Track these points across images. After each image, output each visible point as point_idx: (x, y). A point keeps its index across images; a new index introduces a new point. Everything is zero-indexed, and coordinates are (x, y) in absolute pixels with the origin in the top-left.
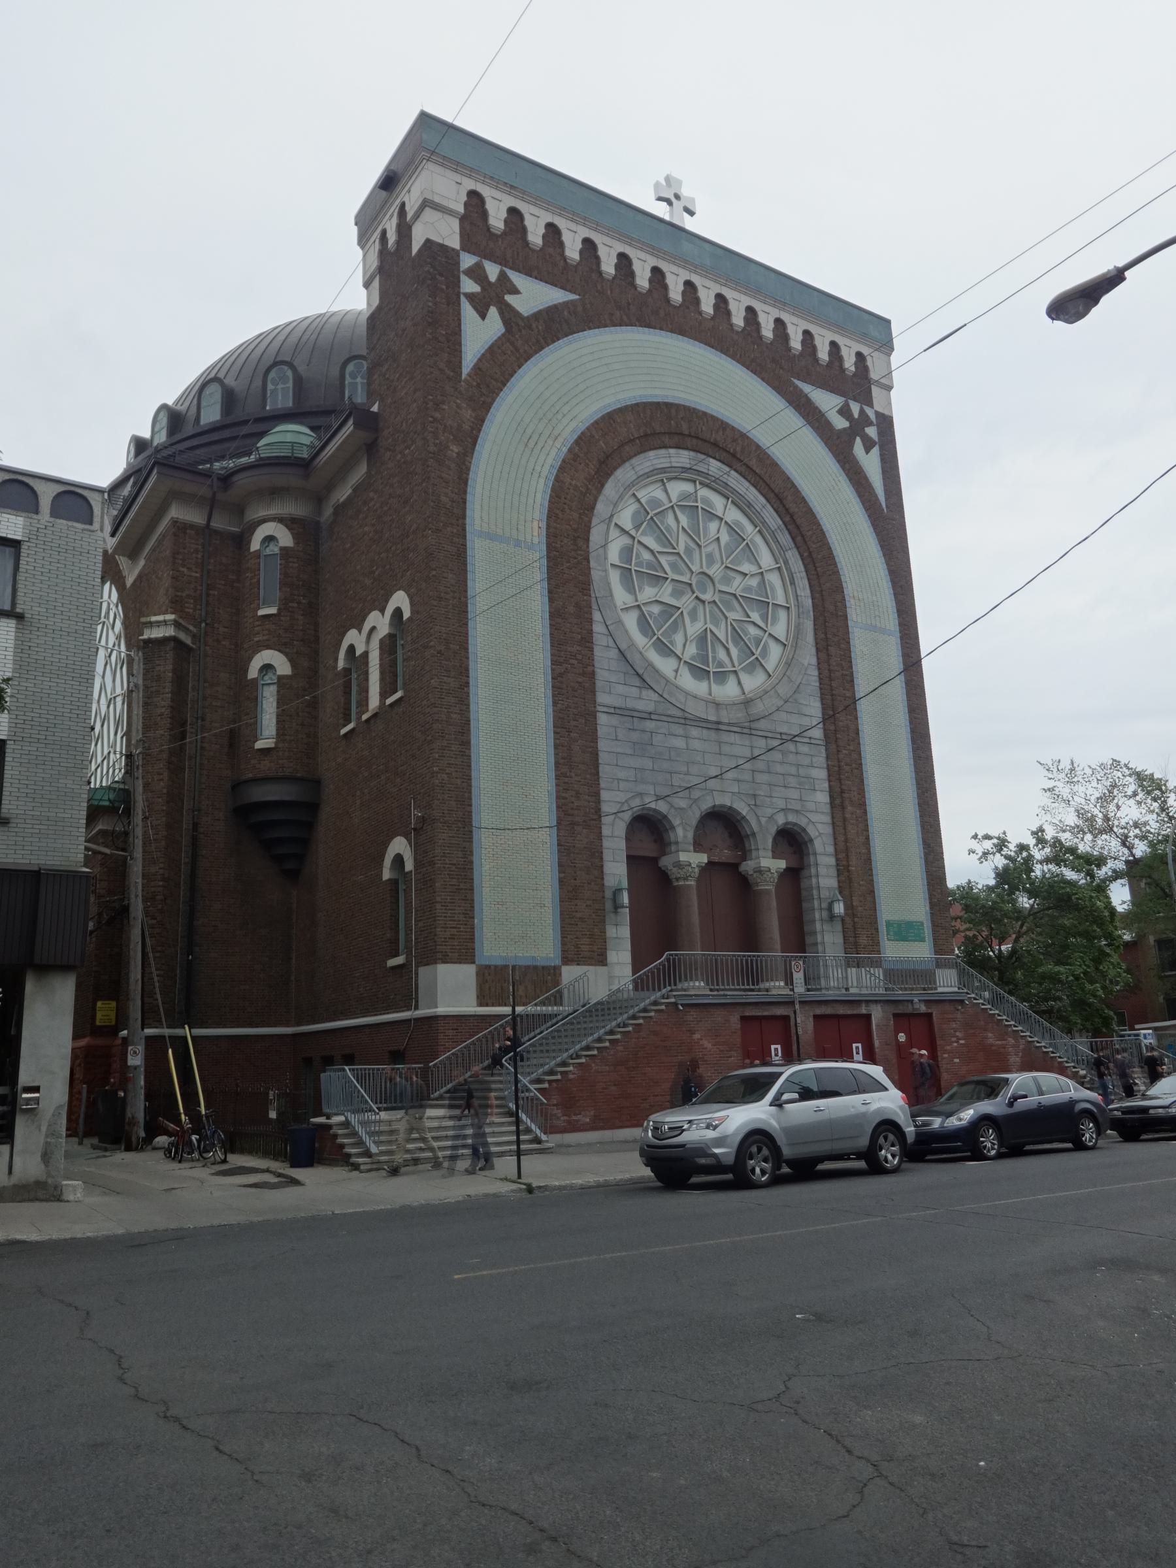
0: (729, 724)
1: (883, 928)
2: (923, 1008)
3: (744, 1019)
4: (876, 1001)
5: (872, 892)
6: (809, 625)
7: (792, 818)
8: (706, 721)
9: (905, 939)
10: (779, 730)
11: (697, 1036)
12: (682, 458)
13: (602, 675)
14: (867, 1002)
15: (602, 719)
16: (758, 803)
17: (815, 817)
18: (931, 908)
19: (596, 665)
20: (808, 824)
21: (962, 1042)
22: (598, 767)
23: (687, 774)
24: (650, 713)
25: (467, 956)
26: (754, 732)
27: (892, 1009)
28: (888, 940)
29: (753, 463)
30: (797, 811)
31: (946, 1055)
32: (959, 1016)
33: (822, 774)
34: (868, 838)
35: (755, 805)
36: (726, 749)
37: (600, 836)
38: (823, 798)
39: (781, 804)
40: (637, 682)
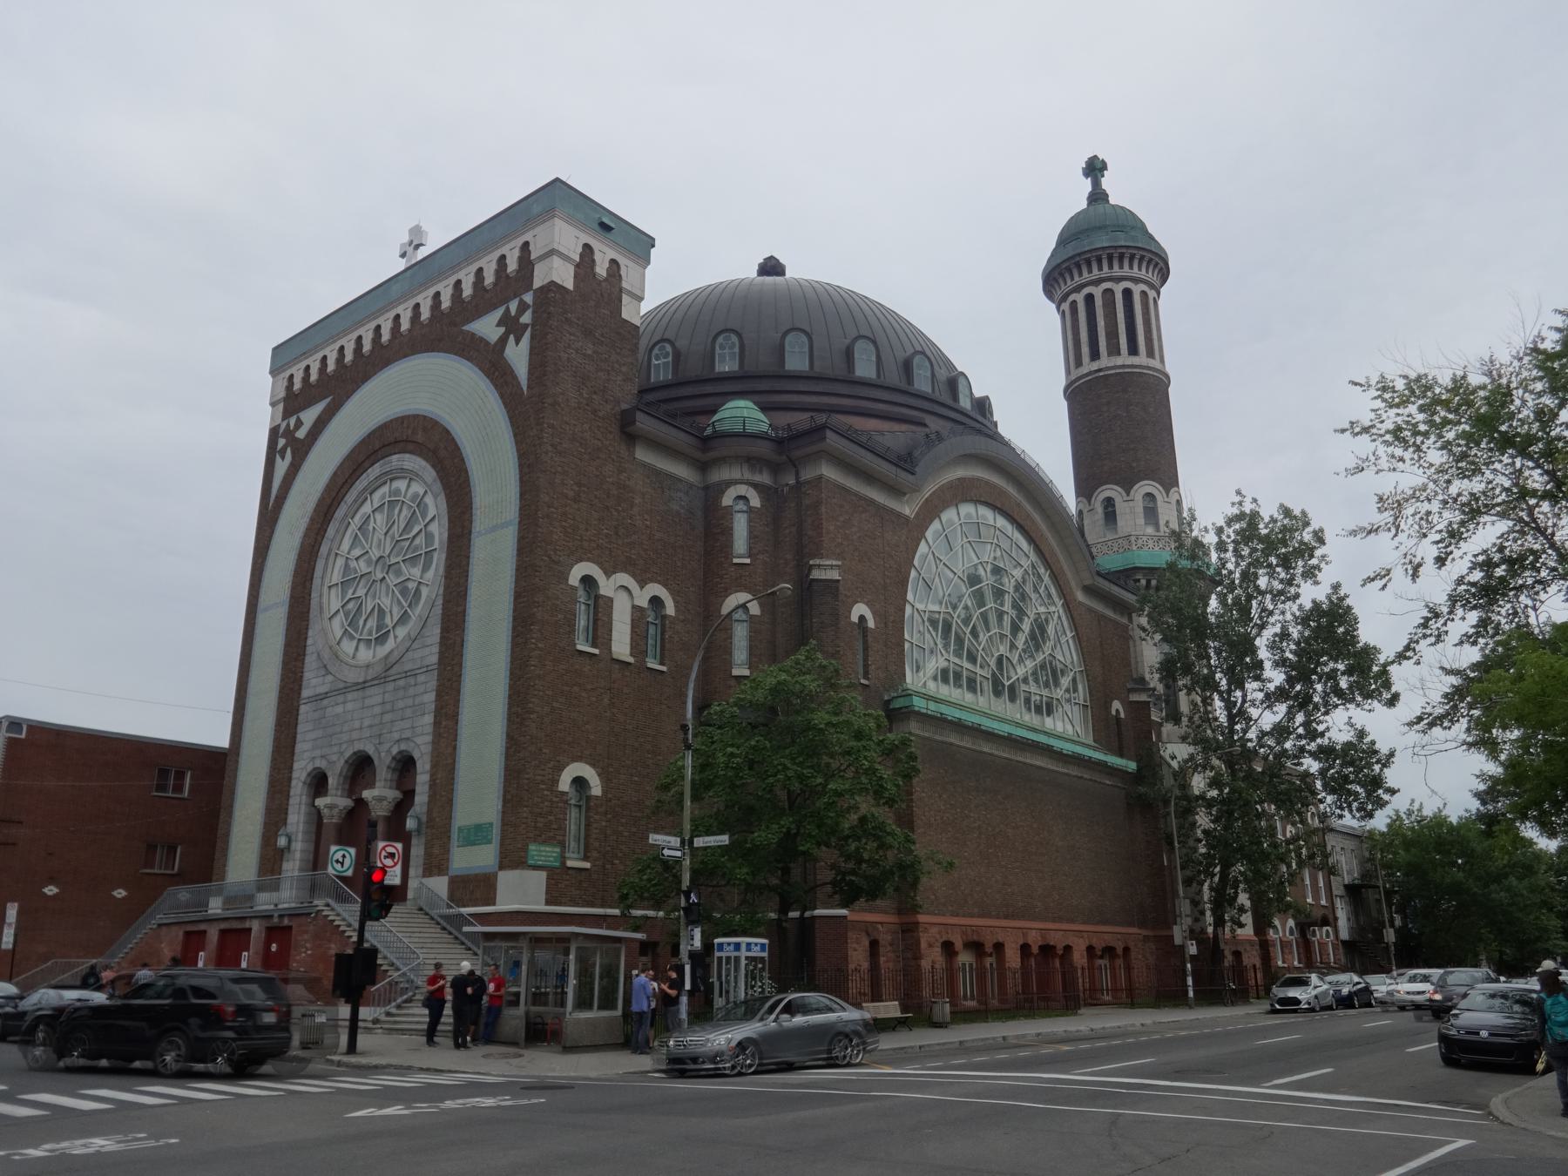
0: (373, 680)
2: (286, 922)
3: (188, 934)
4: (256, 917)
5: (450, 802)
6: (444, 556)
7: (403, 747)
8: (358, 684)
9: (473, 844)
10: (406, 669)
11: (163, 945)
12: (375, 471)
13: (307, 675)
14: (251, 917)
15: (303, 709)
17: (419, 740)
18: (504, 806)
19: (305, 670)
21: (309, 952)
22: (294, 747)
23: (341, 732)
24: (327, 693)
25: (219, 892)
26: (388, 679)
27: (266, 924)
28: (458, 846)
29: (420, 438)
30: (408, 739)
31: (295, 965)
32: (311, 927)
33: (431, 697)
34: (455, 748)
36: (368, 702)
37: (288, 797)
38: (429, 719)
39: (396, 736)
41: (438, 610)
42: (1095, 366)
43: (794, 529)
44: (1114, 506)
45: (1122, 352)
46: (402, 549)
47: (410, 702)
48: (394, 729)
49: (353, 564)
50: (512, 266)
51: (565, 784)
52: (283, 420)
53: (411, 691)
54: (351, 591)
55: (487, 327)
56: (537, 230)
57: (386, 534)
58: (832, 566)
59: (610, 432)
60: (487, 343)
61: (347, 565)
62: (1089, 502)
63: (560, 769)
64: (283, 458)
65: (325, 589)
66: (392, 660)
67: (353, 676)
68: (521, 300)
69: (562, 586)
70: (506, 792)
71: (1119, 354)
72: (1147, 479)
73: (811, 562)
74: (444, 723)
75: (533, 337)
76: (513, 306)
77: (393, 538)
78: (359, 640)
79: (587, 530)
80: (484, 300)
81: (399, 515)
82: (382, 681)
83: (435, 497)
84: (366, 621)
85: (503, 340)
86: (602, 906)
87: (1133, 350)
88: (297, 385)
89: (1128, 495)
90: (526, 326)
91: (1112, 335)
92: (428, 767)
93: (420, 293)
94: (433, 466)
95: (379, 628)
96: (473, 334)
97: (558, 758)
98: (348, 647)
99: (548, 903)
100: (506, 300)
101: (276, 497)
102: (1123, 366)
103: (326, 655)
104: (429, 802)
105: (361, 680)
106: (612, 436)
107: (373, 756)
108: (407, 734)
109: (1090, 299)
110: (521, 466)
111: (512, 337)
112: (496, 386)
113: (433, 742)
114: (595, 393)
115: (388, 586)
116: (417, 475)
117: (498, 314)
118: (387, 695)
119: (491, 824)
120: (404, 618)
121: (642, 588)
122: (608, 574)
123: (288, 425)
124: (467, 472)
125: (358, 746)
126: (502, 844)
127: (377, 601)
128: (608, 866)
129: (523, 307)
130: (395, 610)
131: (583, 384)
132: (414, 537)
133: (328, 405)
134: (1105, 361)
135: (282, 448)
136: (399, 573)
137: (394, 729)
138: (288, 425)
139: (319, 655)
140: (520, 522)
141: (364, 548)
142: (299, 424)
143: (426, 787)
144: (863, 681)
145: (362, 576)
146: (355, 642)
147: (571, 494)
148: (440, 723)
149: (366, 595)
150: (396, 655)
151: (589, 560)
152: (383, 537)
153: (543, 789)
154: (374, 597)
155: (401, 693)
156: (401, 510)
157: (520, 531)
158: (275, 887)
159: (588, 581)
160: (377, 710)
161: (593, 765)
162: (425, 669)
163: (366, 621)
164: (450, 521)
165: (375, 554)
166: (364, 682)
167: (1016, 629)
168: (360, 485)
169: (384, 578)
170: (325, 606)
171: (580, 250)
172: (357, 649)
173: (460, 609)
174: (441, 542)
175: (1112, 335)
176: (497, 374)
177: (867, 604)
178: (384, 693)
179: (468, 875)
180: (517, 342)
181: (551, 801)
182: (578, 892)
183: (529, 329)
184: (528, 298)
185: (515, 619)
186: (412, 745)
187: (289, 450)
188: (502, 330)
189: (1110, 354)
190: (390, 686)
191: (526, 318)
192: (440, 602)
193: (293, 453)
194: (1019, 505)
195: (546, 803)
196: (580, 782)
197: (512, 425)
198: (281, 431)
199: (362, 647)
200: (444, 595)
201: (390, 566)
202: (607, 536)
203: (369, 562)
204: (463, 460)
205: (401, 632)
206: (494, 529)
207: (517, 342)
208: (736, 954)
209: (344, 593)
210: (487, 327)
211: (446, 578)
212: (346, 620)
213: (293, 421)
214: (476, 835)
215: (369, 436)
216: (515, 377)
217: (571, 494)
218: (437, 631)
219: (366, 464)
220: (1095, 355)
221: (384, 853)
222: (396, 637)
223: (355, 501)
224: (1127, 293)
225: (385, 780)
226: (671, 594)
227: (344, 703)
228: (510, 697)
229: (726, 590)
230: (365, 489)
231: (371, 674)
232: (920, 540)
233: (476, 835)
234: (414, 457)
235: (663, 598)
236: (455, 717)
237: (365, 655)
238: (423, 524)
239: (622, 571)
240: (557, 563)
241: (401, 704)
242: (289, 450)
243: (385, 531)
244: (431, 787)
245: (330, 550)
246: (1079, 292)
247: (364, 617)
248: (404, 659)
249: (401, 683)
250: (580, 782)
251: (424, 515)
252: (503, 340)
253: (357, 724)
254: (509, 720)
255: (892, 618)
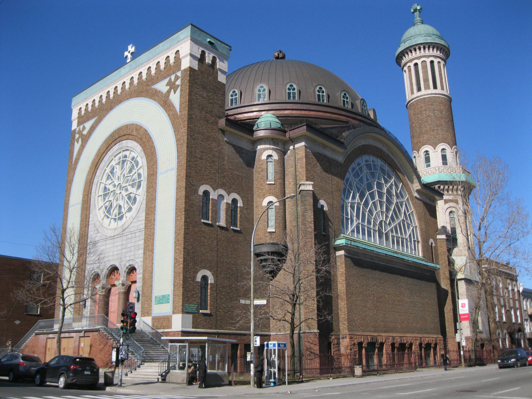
1: (153, 299)
6: (146, 183)
7: (131, 263)
8: (111, 237)
10: (131, 231)
16: (122, 260)
17: (138, 260)
18: (174, 288)
19: (89, 231)
20: (135, 264)
26: (124, 235)
28: (155, 304)
29: (134, 133)
30: (133, 260)
34: (153, 263)
35: (121, 262)
36: (116, 244)
38: (141, 251)
39: (128, 258)
40: (96, 232)
41: (144, 206)
42: (419, 94)
43: (293, 169)
44: (429, 154)
45: (431, 88)
46: (128, 180)
47: (133, 244)
48: (127, 256)
49: (108, 187)
50: (172, 60)
51: (199, 278)
52: (77, 127)
53: (133, 240)
54: (107, 198)
55: (162, 86)
56: (182, 46)
57: (121, 174)
58: (309, 184)
59: (214, 129)
60: (162, 93)
61: (105, 188)
62: (418, 153)
63: (196, 272)
64: (78, 142)
65: (97, 197)
66: (125, 227)
67: (110, 234)
68: (176, 75)
69: (195, 195)
70: (175, 282)
71: (429, 89)
72: (444, 143)
73: (300, 183)
74: (148, 253)
75: (181, 90)
76: (173, 77)
77: (124, 176)
78: (111, 218)
79: (205, 171)
80: (160, 75)
81: (126, 166)
82: (122, 235)
83: (142, 158)
84: (114, 210)
85: (169, 92)
86: (216, 329)
87: (435, 87)
88: (83, 112)
89: (435, 149)
90: (179, 86)
91: (426, 80)
92: (141, 271)
93: (133, 73)
94: (141, 145)
95: (119, 213)
96: (156, 90)
97: (196, 267)
98: (106, 221)
99: (193, 328)
100: (169, 75)
101: (76, 159)
102: (432, 94)
103: (98, 224)
104: (143, 286)
105: (112, 235)
106: (215, 131)
107: (118, 267)
108: (132, 258)
109: (416, 65)
110: (177, 145)
111: (172, 90)
112: (166, 111)
113: (143, 261)
114: (207, 113)
115: (123, 196)
116: (134, 149)
117: (166, 81)
118: (123, 241)
119: (169, 295)
120: (130, 209)
121: (229, 195)
122: (214, 189)
123: (80, 129)
124: (155, 148)
125: (112, 263)
126: (174, 302)
127: (118, 202)
128: (218, 313)
129: (177, 78)
130: (126, 205)
131: (203, 109)
132: (133, 175)
133: (96, 120)
134: (423, 92)
135: (77, 138)
136: (127, 190)
137: (127, 256)
138: (80, 129)
139: (95, 224)
140: (177, 169)
141: (112, 180)
142: (84, 128)
143: (141, 280)
144: (323, 233)
145: (112, 192)
146: (110, 219)
147: (199, 156)
148: (146, 253)
149: (113, 199)
150: (127, 225)
151: (206, 184)
152: (120, 175)
153: (190, 281)
154: (117, 200)
155: (129, 241)
156: (127, 164)
157: (178, 172)
158: (80, 320)
159: (206, 193)
160: (120, 248)
161: (211, 271)
162: (139, 231)
163: (114, 210)
164: (148, 169)
165: (117, 183)
166: (114, 236)
167: (388, 210)
168: (110, 153)
169: (121, 192)
170: (97, 204)
171: (200, 53)
172: (110, 222)
173: (153, 205)
174: (144, 177)
175: (426, 80)
176: (166, 106)
177: (324, 200)
178: (122, 240)
179: (160, 317)
180: (175, 92)
181: (194, 286)
182: (205, 323)
183: (180, 87)
184: (179, 74)
185: (176, 209)
186: (135, 262)
187: (80, 139)
188: (168, 87)
189: (426, 89)
190: (125, 238)
191: (178, 82)
192: (145, 202)
193: (82, 141)
194: (388, 156)
195: (191, 286)
196: (205, 278)
197: (173, 127)
198: (77, 131)
199: (112, 221)
200: (146, 200)
201: (123, 187)
202: (214, 173)
203: (115, 186)
204: (153, 143)
205: (128, 215)
206: (167, 171)
207: (175, 92)
208: (274, 348)
209: (104, 199)
210: (162, 86)
211: (147, 192)
212: (106, 210)
213: (81, 127)
214: (162, 300)
215: (113, 133)
216: (174, 107)
217: (199, 156)
218: (144, 214)
219: (112, 145)
220: (419, 89)
221: (129, 307)
222: (126, 217)
223: (108, 160)
224: (432, 62)
225: (124, 277)
226: (241, 197)
227: (106, 245)
228: (175, 242)
229: (264, 195)
230: (112, 155)
231: (117, 232)
232: (347, 172)
233: (162, 300)
234: (132, 141)
235: (238, 199)
236: (152, 251)
237: (114, 224)
238: (137, 169)
239: (220, 188)
240: (194, 185)
241: (129, 245)
242: (80, 139)
243: (120, 173)
244: (143, 280)
245: (98, 181)
246: (411, 62)
247: (113, 209)
248: (130, 226)
249: (129, 236)
250: (205, 278)
251: (137, 166)
252: (169, 92)
253: (111, 254)
254: (175, 252)
255: (335, 206)
